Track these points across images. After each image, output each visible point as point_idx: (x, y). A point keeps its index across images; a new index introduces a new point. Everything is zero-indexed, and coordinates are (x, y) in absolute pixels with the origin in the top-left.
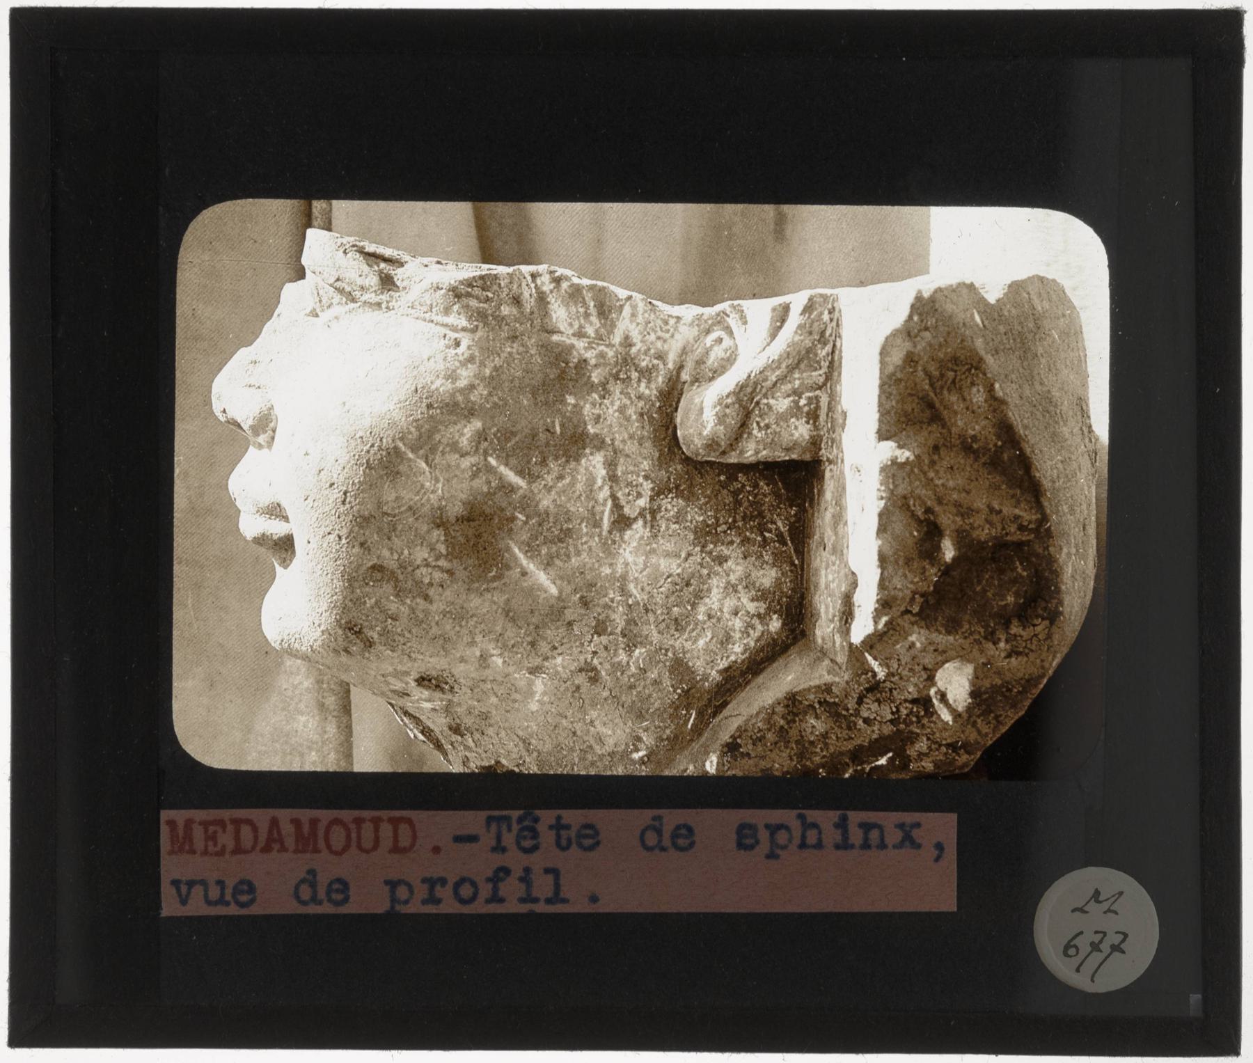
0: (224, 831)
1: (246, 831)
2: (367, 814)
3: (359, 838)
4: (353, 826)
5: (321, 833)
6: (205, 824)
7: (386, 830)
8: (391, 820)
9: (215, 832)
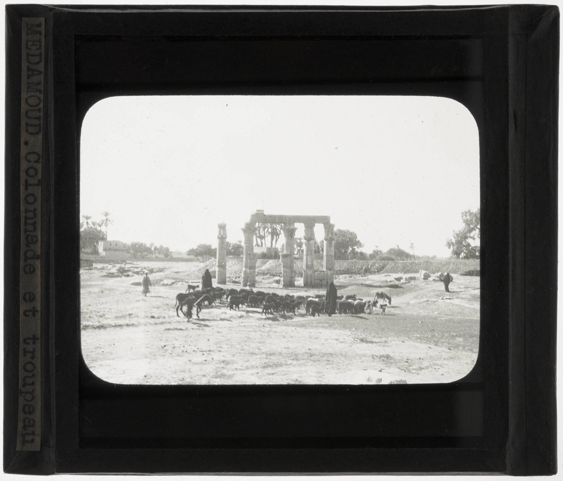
0: (37, 49)
1: (37, 59)
2: (42, 114)
3: (33, 110)
4: (37, 108)
5: (33, 94)
6: (40, 41)
7: (36, 122)
8: (40, 124)
9: (36, 45)
